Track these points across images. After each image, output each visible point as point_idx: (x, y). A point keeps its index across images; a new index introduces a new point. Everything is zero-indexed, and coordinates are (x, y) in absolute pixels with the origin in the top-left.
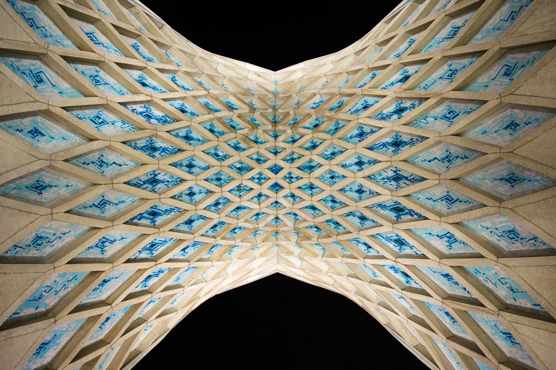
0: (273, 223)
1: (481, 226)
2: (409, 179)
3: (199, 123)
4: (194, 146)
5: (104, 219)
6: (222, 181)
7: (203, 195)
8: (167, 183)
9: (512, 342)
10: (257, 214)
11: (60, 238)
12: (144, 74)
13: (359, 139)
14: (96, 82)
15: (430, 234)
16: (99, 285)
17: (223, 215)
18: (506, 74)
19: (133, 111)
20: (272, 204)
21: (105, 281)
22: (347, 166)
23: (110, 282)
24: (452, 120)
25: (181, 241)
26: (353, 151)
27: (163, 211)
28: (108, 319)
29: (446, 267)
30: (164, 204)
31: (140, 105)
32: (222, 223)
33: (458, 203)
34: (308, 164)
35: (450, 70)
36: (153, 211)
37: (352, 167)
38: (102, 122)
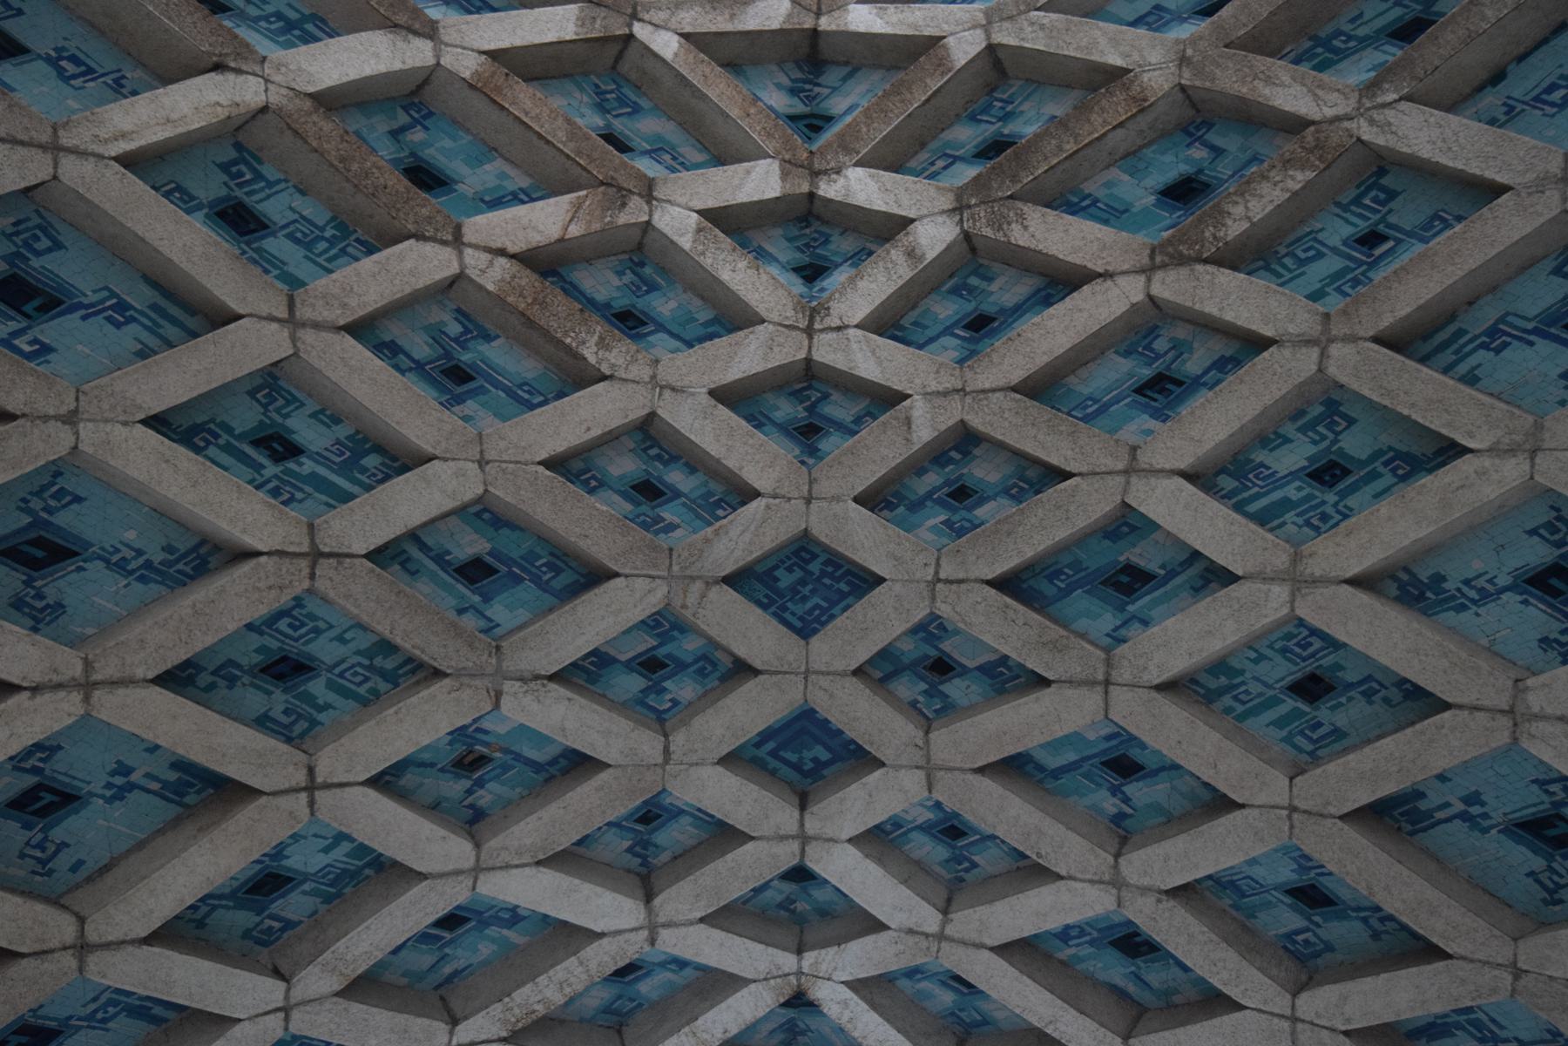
3: (129, 162)
6: (317, 687)
7: (147, 809)
17: (316, 980)
26: (1512, 471)
37: (1490, 611)
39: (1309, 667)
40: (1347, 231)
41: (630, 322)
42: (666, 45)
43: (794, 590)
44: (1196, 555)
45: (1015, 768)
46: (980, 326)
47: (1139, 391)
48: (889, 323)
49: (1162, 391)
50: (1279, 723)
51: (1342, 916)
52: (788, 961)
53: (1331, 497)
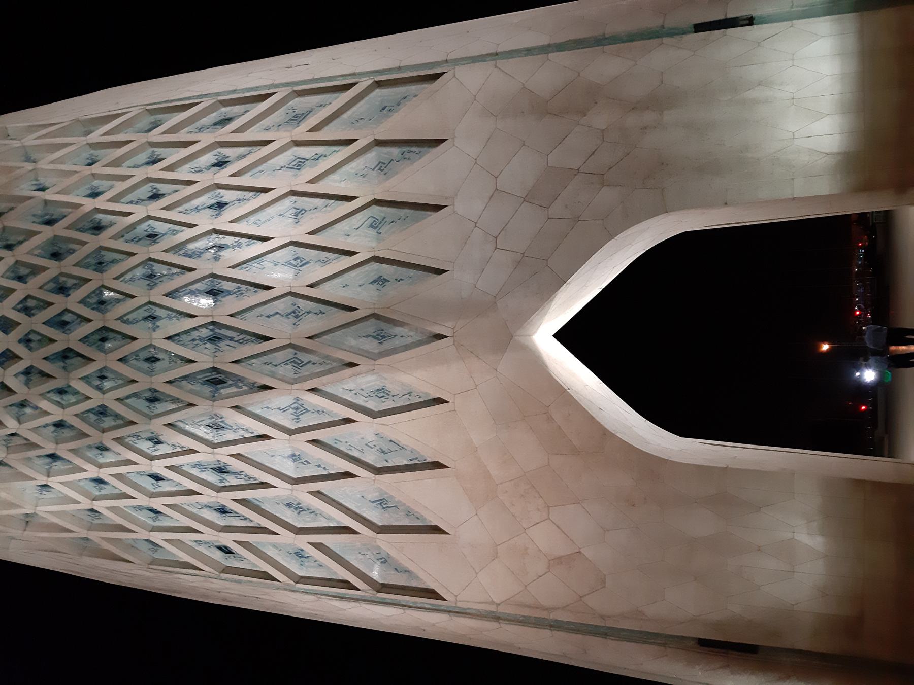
9: (384, 508)
13: (148, 282)
15: (268, 408)
18: (371, 226)
29: (300, 442)
33: (310, 365)
34: (58, 319)
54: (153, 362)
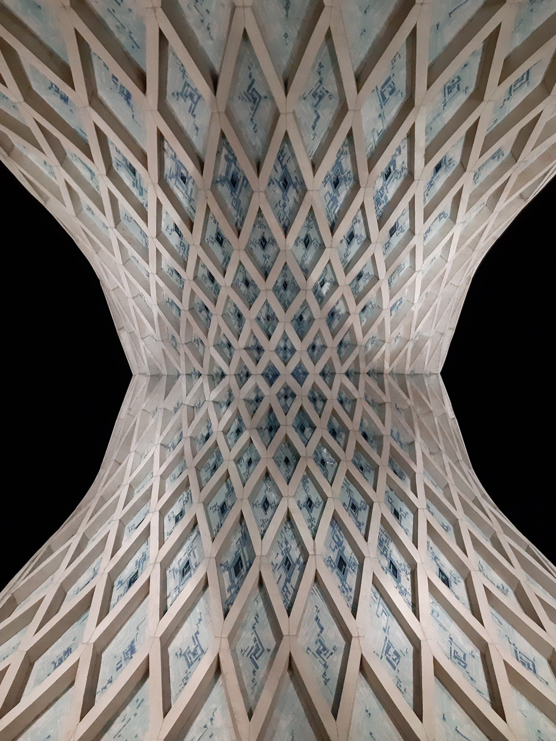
0: (215, 370)
1: (216, 709)
2: (288, 584)
4: (338, 249)
5: (230, 99)
8: (281, 204)
10: (229, 345)
11: (202, 21)
12: (454, 168)
13: (347, 504)
14: (449, 87)
15: (200, 620)
16: (121, 86)
19: (399, 150)
20: (245, 367)
21: (128, 97)
22: (304, 485)
23: (127, 106)
24: (384, 658)
25: (191, 226)
27: (238, 196)
28: (65, 99)
30: (250, 199)
31: (406, 161)
32: (217, 290)
33: (252, 667)
34: (306, 423)
35: (465, 655)
36: (239, 180)
38: (384, 98)
39: (290, 460)
40: (362, 464)
41: (341, 343)
42: (383, 348)
43: (298, 372)
44: (308, 441)
45: (271, 410)
46: (341, 402)
47: (333, 429)
48: (342, 387)
49: (334, 433)
50: (281, 456)
51: (247, 468)
52: (233, 372)
53: (319, 463)
54: (264, 506)
